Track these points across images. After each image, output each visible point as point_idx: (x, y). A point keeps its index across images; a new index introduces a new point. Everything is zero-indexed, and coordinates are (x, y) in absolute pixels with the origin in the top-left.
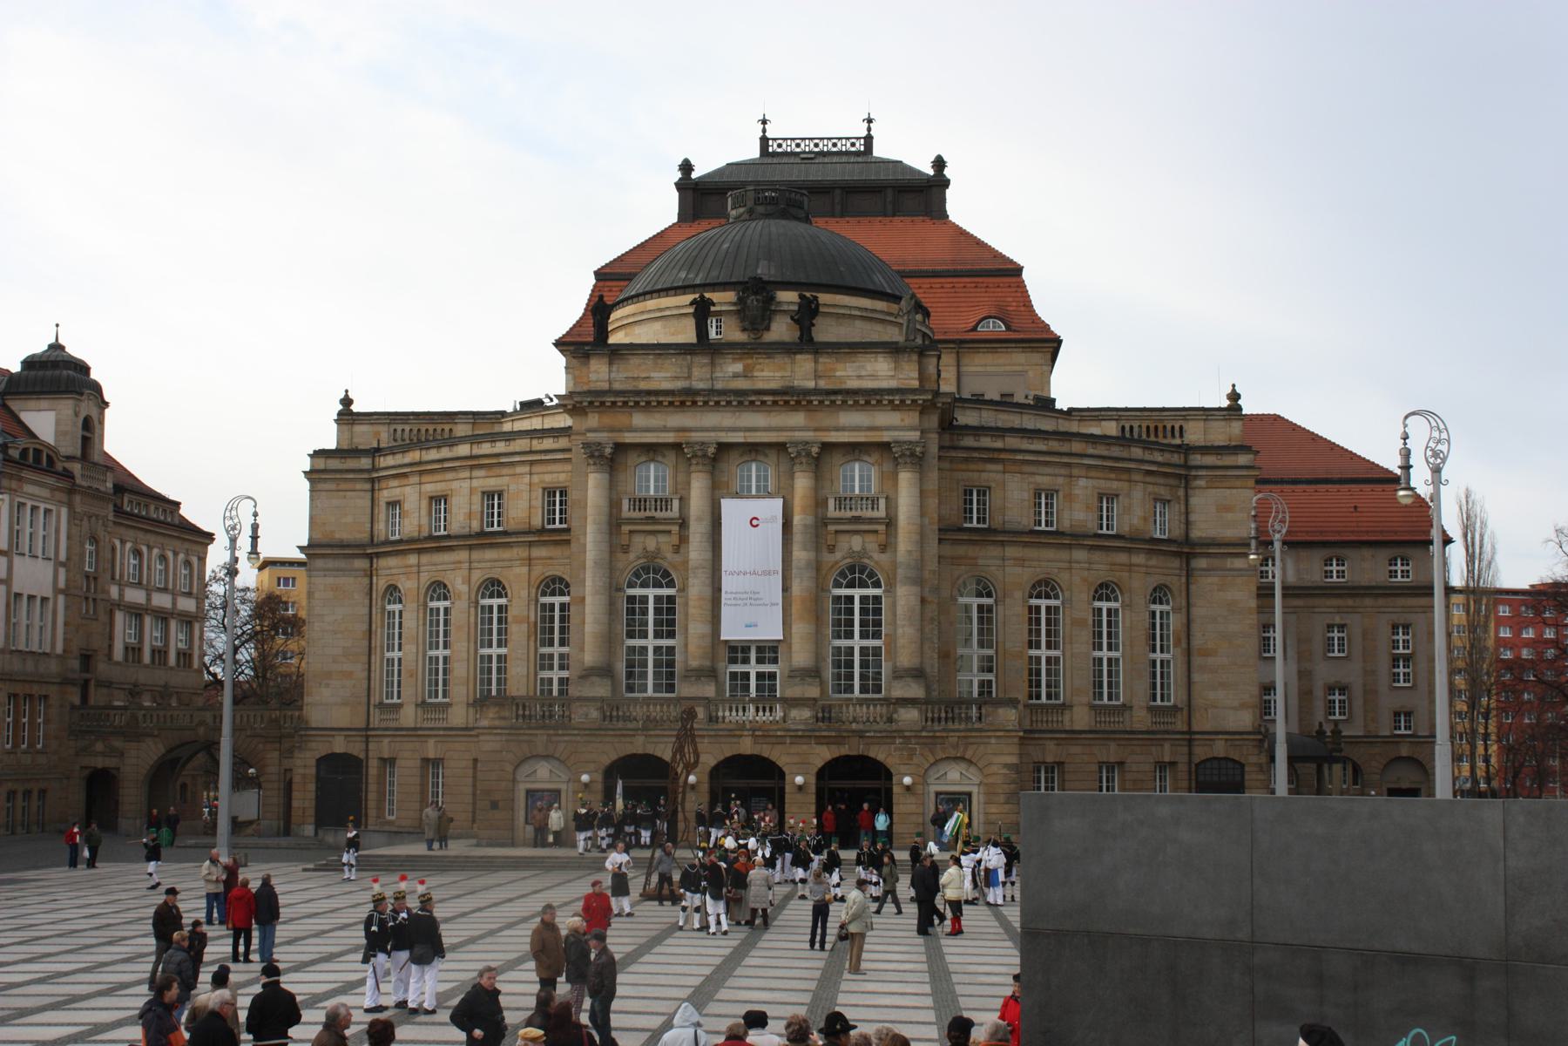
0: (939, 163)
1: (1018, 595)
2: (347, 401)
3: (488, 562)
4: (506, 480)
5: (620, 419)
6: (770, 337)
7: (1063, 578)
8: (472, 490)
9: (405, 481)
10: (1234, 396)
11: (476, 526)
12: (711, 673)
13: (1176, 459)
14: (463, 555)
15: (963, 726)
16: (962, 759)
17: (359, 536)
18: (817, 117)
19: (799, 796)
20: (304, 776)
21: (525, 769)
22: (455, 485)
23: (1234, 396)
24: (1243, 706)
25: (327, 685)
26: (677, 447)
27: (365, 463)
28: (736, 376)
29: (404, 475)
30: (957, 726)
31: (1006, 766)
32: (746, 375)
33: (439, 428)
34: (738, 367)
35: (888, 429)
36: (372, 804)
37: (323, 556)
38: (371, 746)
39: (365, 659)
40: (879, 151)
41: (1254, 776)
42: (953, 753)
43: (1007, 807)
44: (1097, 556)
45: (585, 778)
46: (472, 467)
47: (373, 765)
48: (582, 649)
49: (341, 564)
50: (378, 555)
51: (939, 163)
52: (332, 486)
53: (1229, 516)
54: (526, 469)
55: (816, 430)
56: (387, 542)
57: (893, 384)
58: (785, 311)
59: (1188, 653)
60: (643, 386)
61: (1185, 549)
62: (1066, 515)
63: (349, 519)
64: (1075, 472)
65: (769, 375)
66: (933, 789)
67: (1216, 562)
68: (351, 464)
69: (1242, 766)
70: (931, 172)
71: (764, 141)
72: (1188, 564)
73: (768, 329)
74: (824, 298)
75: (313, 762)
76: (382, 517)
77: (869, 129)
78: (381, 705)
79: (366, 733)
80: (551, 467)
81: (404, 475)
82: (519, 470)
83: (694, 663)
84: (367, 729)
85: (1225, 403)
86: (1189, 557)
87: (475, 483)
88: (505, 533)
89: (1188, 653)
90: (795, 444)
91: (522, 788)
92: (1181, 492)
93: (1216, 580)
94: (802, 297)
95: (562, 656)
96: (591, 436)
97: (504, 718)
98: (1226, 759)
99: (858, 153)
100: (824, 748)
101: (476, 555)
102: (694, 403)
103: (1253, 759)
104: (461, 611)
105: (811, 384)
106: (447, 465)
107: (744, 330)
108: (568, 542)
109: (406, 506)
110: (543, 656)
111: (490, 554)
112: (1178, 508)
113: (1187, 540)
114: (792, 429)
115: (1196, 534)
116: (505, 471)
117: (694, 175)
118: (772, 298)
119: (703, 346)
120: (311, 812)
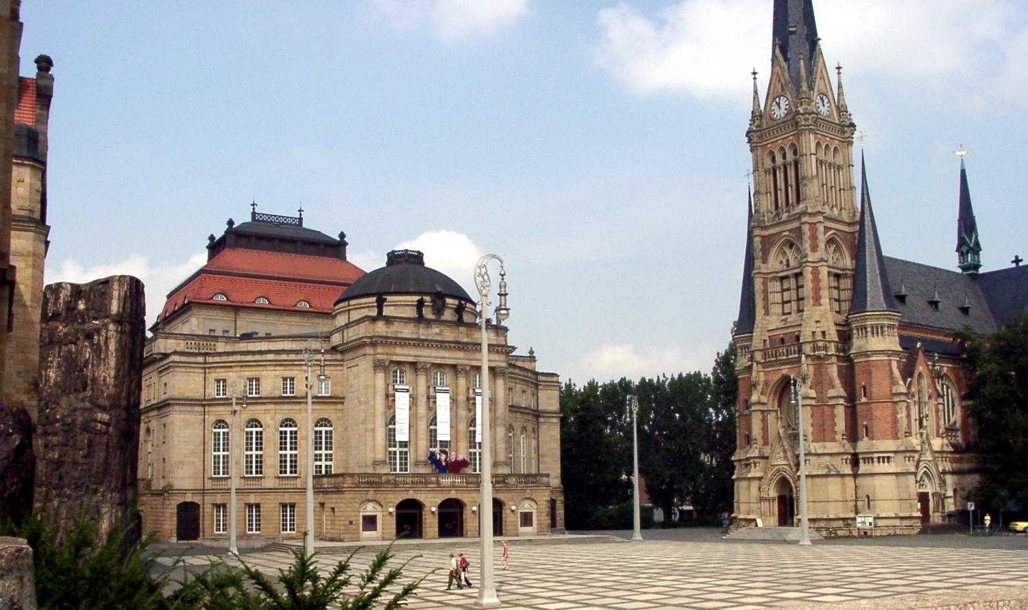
0: (342, 235)
3: (287, 411)
5: (391, 350)
6: (443, 318)
9: (230, 370)
10: (531, 352)
13: (533, 376)
16: (529, 498)
18: (279, 206)
20: (171, 513)
22: (264, 373)
23: (531, 352)
24: (556, 477)
25: (182, 468)
26: (413, 364)
27: (200, 359)
28: (436, 334)
29: (231, 367)
32: (440, 334)
33: (209, 343)
34: (437, 330)
35: (494, 361)
37: (180, 404)
38: (205, 498)
40: (305, 225)
42: (528, 496)
43: (547, 518)
49: (189, 408)
51: (342, 235)
52: (183, 370)
53: (551, 401)
55: (468, 360)
56: (215, 399)
57: (495, 343)
58: (450, 308)
59: (538, 455)
60: (399, 335)
61: (537, 414)
62: (514, 399)
63: (192, 386)
64: (517, 381)
65: (449, 335)
66: (520, 511)
67: (546, 420)
68: (192, 359)
70: (338, 239)
71: (254, 214)
73: (443, 314)
74: (468, 305)
75: (175, 506)
77: (301, 215)
78: (211, 478)
79: (203, 492)
81: (231, 367)
84: (204, 490)
85: (528, 355)
86: (538, 417)
87: (277, 373)
88: (260, 398)
89: (538, 455)
90: (461, 365)
94: (460, 303)
95: (326, 455)
96: (379, 357)
99: (295, 225)
101: (278, 407)
102: (423, 345)
104: (271, 436)
105: (465, 340)
106: (260, 363)
107: (434, 314)
108: (343, 403)
109: (229, 382)
110: (316, 455)
113: (537, 411)
114: (459, 359)
116: (295, 368)
117: (234, 226)
118: (444, 302)
119: (420, 319)
120: (175, 531)
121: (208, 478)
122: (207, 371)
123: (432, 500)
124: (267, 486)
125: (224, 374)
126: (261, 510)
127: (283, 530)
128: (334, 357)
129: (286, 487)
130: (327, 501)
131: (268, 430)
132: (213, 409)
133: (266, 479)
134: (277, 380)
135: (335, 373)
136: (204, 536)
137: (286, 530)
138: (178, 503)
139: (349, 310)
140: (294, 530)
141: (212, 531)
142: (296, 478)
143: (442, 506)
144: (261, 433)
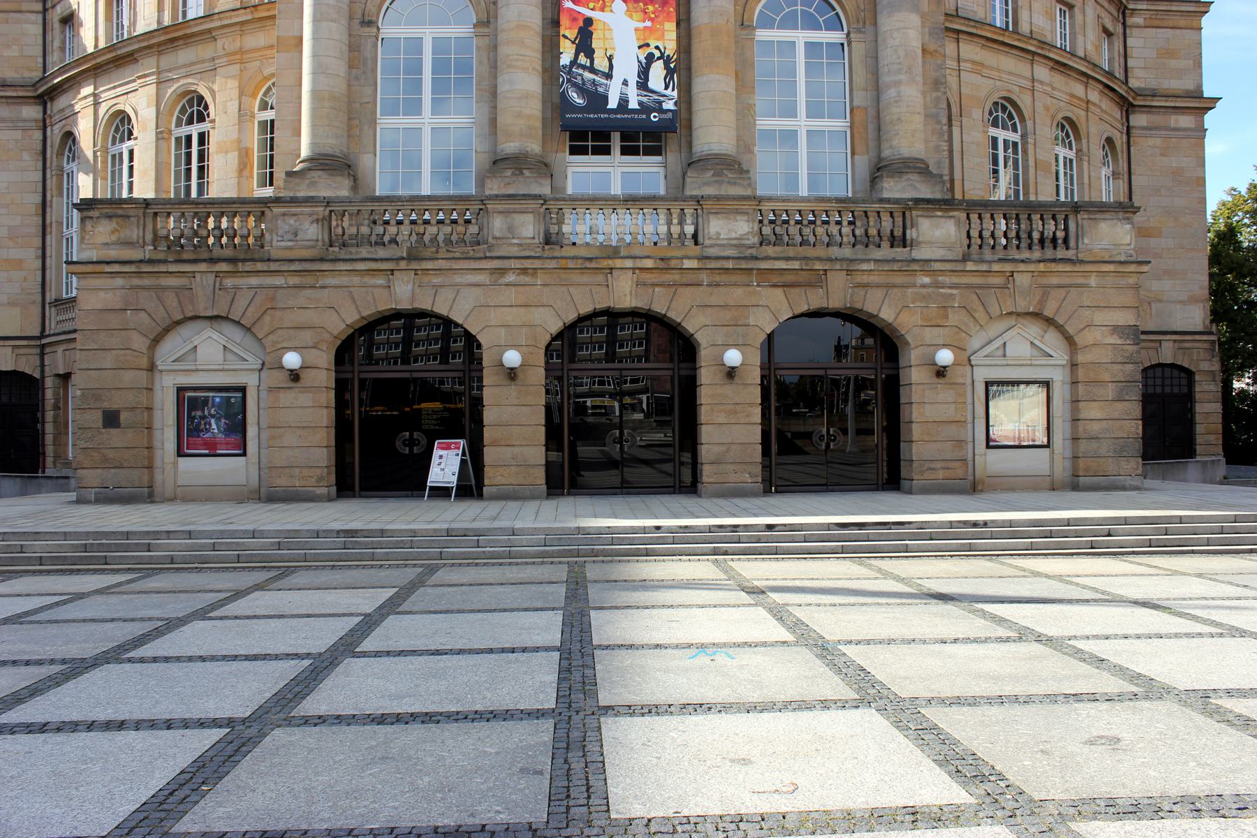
1: (977, 114)
7: (1024, 101)
11: (167, 21)
12: (544, 167)
15: (1037, 254)
16: (1036, 315)
17: (27, 74)
19: (728, 390)
21: (171, 348)
24: (1193, 300)
30: (1025, 254)
31: (1116, 329)
36: (49, 439)
39: (38, 242)
41: (1206, 388)
42: (1023, 305)
44: (1058, 79)
45: (292, 360)
47: (49, 382)
48: (298, 133)
53: (1173, 63)
66: (982, 375)
67: (1158, 119)
69: (1189, 374)
72: (1128, 120)
76: (57, 44)
79: (41, 343)
83: (510, 147)
84: (43, 335)
91: (166, 385)
92: (1120, 29)
93: (1158, 141)
97: (129, 244)
98: (1173, 366)
100: (779, 291)
101: (167, 60)
103: (1205, 366)
112: (1118, 45)
115: (1133, 83)
123: (514, 316)
143: (565, 346)
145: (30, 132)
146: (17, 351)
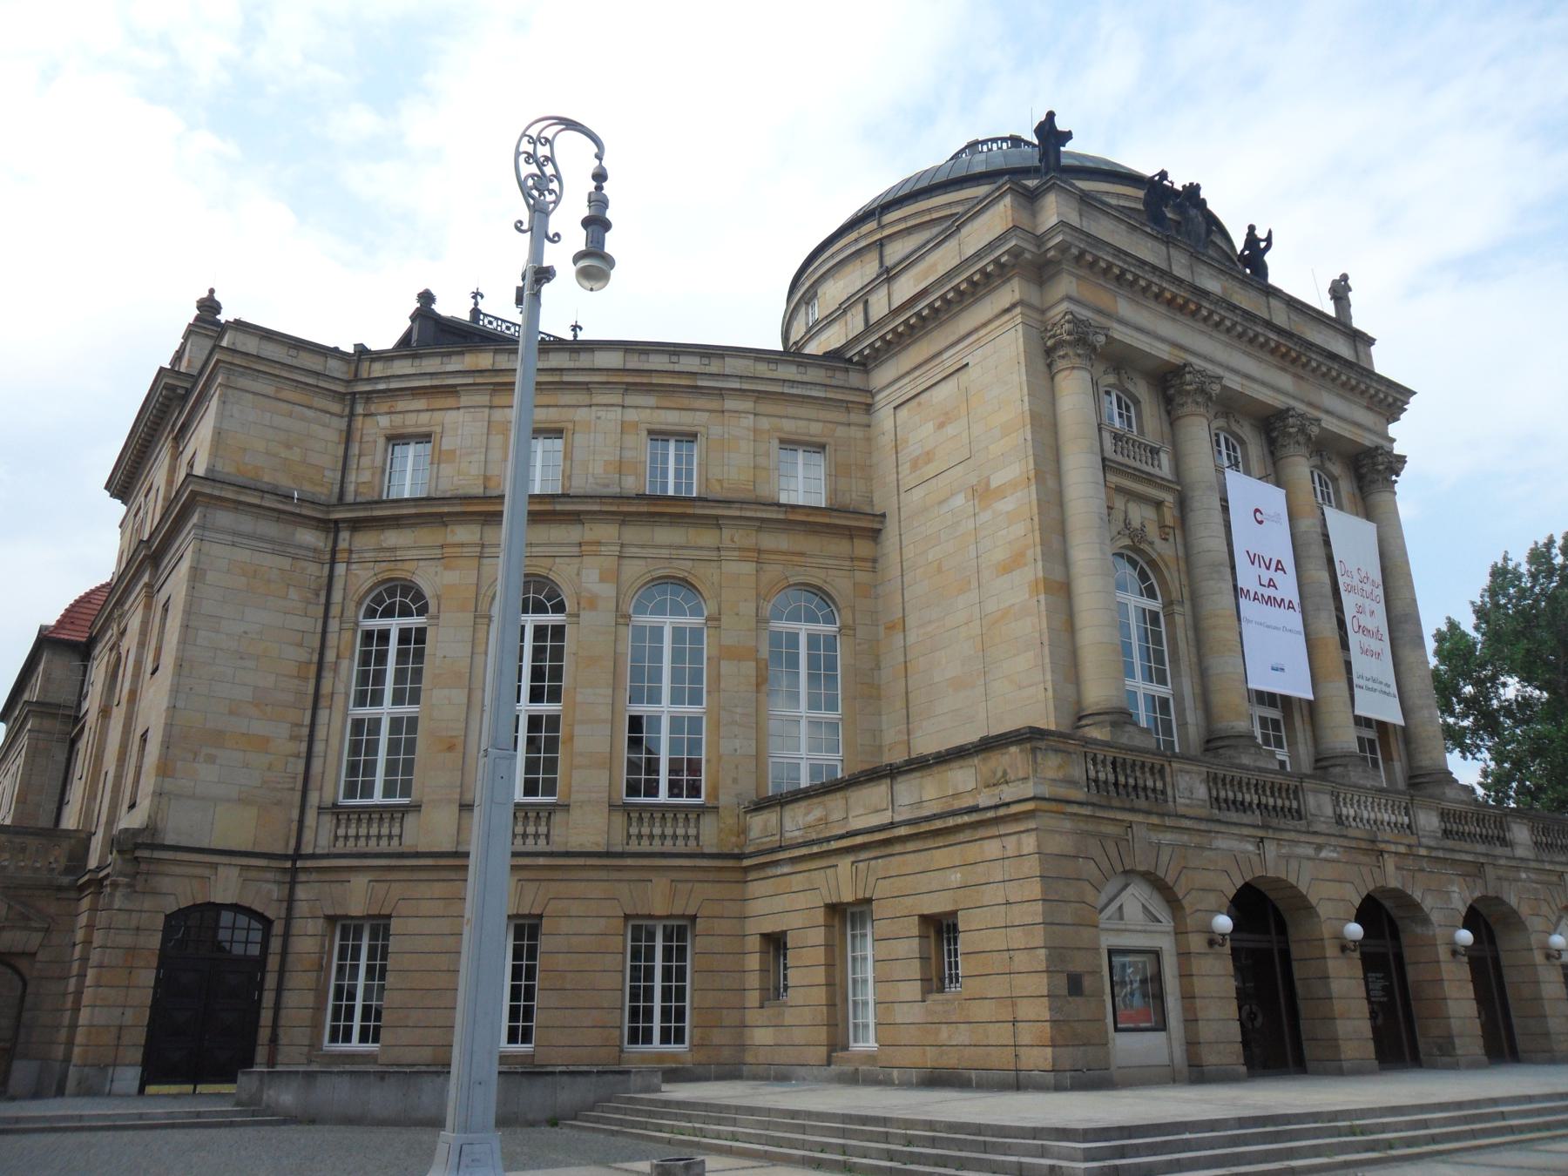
2: (209, 306)
4: (701, 417)
8: (624, 427)
14: (606, 532)
20: (132, 951)
22: (581, 414)
25: (211, 759)
38: (301, 893)
46: (629, 388)
50: (356, 525)
54: (748, 405)
71: (476, 312)
78: (335, 810)
79: (292, 864)
80: (792, 410)
82: (730, 404)
84: (297, 855)
87: (631, 415)
101: (632, 534)
111: (665, 535)
120: (140, 1036)
121: (321, 809)
122: (360, 409)
124: (574, 846)
125: (424, 417)
126: (544, 944)
127: (633, 1039)
128: (839, 378)
129: (656, 847)
130: (882, 889)
131: (586, 616)
132: (366, 541)
133: (575, 813)
134: (630, 440)
135: (841, 431)
136: (271, 1062)
137: (648, 1039)
138: (171, 906)
139: (881, 244)
140: (680, 1039)
141: (315, 1044)
142: (701, 810)
144: (559, 632)
145: (306, 564)
146: (253, 874)
